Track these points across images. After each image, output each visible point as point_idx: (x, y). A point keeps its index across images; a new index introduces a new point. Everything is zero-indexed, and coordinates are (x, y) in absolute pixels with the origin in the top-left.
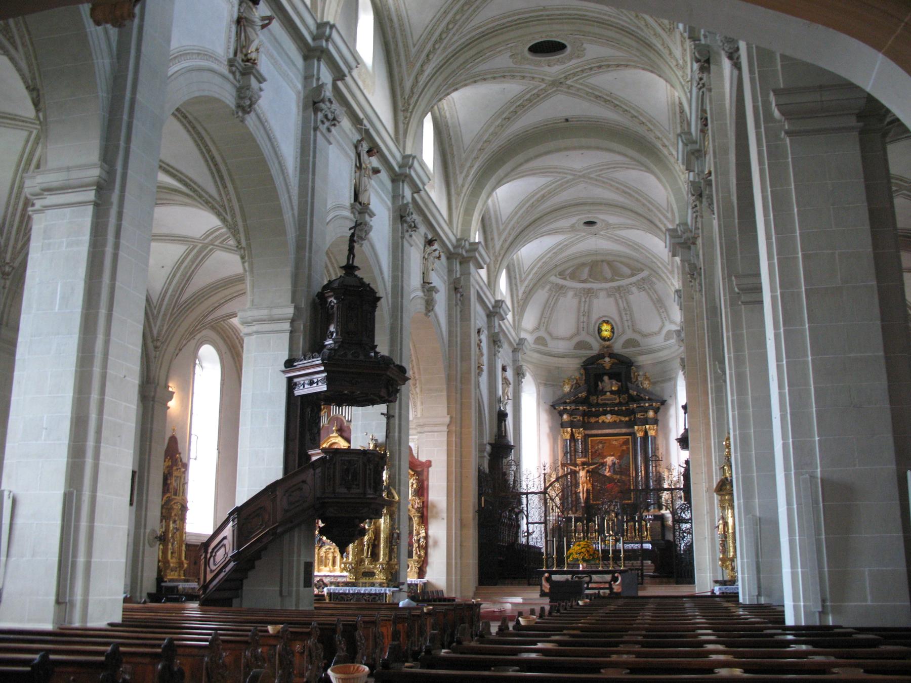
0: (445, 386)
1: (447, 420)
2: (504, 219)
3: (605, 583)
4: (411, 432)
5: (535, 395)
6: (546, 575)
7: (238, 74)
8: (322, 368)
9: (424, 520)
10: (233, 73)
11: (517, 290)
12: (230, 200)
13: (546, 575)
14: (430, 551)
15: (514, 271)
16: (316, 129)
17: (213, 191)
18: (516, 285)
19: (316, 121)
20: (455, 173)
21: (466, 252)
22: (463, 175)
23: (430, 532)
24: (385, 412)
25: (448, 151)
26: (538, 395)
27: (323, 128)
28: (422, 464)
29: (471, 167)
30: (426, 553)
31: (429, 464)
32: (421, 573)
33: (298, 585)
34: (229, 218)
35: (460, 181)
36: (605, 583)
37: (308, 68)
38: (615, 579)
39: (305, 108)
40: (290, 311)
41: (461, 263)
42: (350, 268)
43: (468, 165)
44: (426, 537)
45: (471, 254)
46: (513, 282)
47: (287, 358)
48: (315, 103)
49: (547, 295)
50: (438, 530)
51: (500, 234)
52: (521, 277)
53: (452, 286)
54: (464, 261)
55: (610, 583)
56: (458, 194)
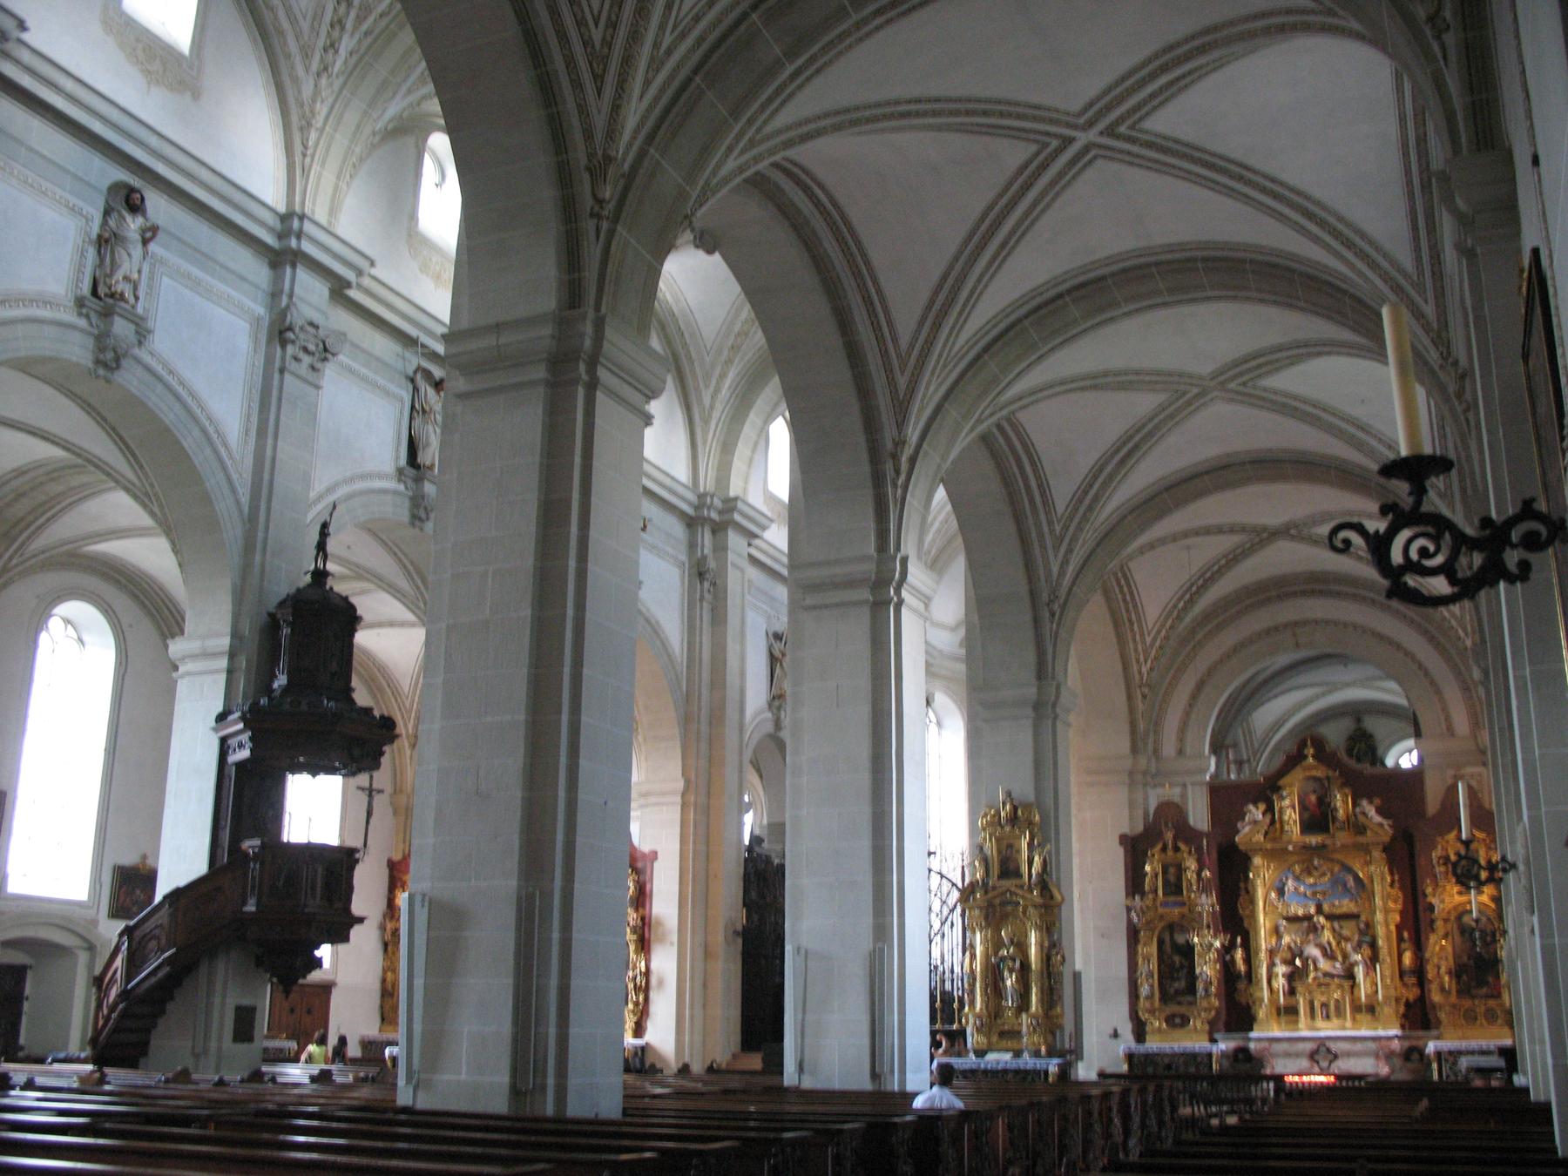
0: (676, 731)
1: (680, 785)
4: (633, 805)
7: (93, 316)
8: (241, 726)
9: (644, 945)
10: (87, 317)
12: (152, 486)
14: (652, 995)
16: (282, 371)
17: (130, 475)
19: (283, 359)
20: (697, 388)
21: (720, 513)
22: (712, 389)
23: (654, 965)
24: (367, 785)
25: (682, 352)
27: (303, 369)
28: (644, 855)
29: (722, 376)
30: (646, 999)
31: (654, 856)
32: (639, 1031)
33: (220, 1039)
34: (156, 510)
35: (707, 401)
37: (277, 281)
39: (269, 341)
40: (225, 642)
41: (714, 532)
42: (320, 576)
43: (717, 372)
44: (647, 974)
45: (726, 517)
47: (220, 709)
48: (281, 332)
50: (664, 962)
53: (695, 570)
54: (719, 529)
56: (706, 422)
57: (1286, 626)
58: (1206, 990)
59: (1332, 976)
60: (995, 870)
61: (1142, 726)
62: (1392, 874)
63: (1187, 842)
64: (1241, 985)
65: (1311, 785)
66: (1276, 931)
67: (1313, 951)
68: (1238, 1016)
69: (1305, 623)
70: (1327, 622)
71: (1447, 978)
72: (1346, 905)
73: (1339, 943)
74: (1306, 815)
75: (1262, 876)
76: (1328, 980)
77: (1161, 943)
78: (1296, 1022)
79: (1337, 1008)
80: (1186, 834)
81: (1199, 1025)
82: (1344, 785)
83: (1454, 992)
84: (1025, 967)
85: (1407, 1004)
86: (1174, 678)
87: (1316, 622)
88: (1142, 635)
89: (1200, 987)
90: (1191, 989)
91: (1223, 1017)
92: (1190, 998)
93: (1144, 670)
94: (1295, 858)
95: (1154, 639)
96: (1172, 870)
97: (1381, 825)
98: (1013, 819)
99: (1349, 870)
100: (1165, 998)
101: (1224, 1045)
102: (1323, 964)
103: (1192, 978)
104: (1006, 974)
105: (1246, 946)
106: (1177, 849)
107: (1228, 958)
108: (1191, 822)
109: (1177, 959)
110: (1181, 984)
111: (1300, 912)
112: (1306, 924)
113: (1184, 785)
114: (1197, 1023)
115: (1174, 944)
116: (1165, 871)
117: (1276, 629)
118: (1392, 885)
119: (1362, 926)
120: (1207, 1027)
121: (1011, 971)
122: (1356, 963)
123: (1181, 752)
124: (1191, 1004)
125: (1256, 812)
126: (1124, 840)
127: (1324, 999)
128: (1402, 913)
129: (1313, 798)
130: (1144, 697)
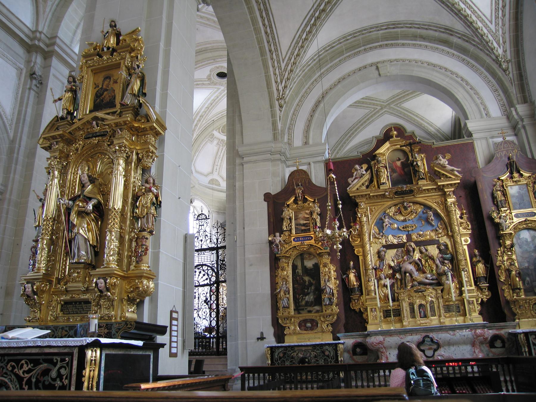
45: (50, 49)
49: (216, 149)
54: (47, 55)
57: (371, 65)
58: (330, 299)
59: (425, 284)
61: (279, 125)
62: (461, 209)
63: (311, 196)
64: (355, 297)
66: (380, 256)
70: (397, 60)
71: (517, 279)
72: (429, 234)
73: (426, 261)
74: (395, 175)
75: (367, 216)
76: (422, 287)
77: (294, 267)
79: (432, 308)
80: (310, 188)
81: (324, 326)
82: (420, 152)
83: (522, 290)
85: (482, 303)
88: (279, 62)
89: (325, 297)
90: (318, 301)
91: (343, 321)
92: (317, 308)
93: (280, 88)
95: (287, 65)
97: (453, 170)
99: (430, 208)
100: (298, 309)
103: (319, 291)
105: (357, 267)
106: (305, 200)
107: (344, 277)
108: (314, 182)
109: (307, 279)
110: (310, 298)
111: (395, 241)
113: (309, 164)
115: (304, 268)
117: (365, 67)
118: (461, 218)
119: (443, 247)
120: (330, 328)
122: (445, 273)
123: (306, 143)
124: (317, 311)
126: (267, 197)
128: (472, 236)
129: (399, 163)
130: (281, 106)
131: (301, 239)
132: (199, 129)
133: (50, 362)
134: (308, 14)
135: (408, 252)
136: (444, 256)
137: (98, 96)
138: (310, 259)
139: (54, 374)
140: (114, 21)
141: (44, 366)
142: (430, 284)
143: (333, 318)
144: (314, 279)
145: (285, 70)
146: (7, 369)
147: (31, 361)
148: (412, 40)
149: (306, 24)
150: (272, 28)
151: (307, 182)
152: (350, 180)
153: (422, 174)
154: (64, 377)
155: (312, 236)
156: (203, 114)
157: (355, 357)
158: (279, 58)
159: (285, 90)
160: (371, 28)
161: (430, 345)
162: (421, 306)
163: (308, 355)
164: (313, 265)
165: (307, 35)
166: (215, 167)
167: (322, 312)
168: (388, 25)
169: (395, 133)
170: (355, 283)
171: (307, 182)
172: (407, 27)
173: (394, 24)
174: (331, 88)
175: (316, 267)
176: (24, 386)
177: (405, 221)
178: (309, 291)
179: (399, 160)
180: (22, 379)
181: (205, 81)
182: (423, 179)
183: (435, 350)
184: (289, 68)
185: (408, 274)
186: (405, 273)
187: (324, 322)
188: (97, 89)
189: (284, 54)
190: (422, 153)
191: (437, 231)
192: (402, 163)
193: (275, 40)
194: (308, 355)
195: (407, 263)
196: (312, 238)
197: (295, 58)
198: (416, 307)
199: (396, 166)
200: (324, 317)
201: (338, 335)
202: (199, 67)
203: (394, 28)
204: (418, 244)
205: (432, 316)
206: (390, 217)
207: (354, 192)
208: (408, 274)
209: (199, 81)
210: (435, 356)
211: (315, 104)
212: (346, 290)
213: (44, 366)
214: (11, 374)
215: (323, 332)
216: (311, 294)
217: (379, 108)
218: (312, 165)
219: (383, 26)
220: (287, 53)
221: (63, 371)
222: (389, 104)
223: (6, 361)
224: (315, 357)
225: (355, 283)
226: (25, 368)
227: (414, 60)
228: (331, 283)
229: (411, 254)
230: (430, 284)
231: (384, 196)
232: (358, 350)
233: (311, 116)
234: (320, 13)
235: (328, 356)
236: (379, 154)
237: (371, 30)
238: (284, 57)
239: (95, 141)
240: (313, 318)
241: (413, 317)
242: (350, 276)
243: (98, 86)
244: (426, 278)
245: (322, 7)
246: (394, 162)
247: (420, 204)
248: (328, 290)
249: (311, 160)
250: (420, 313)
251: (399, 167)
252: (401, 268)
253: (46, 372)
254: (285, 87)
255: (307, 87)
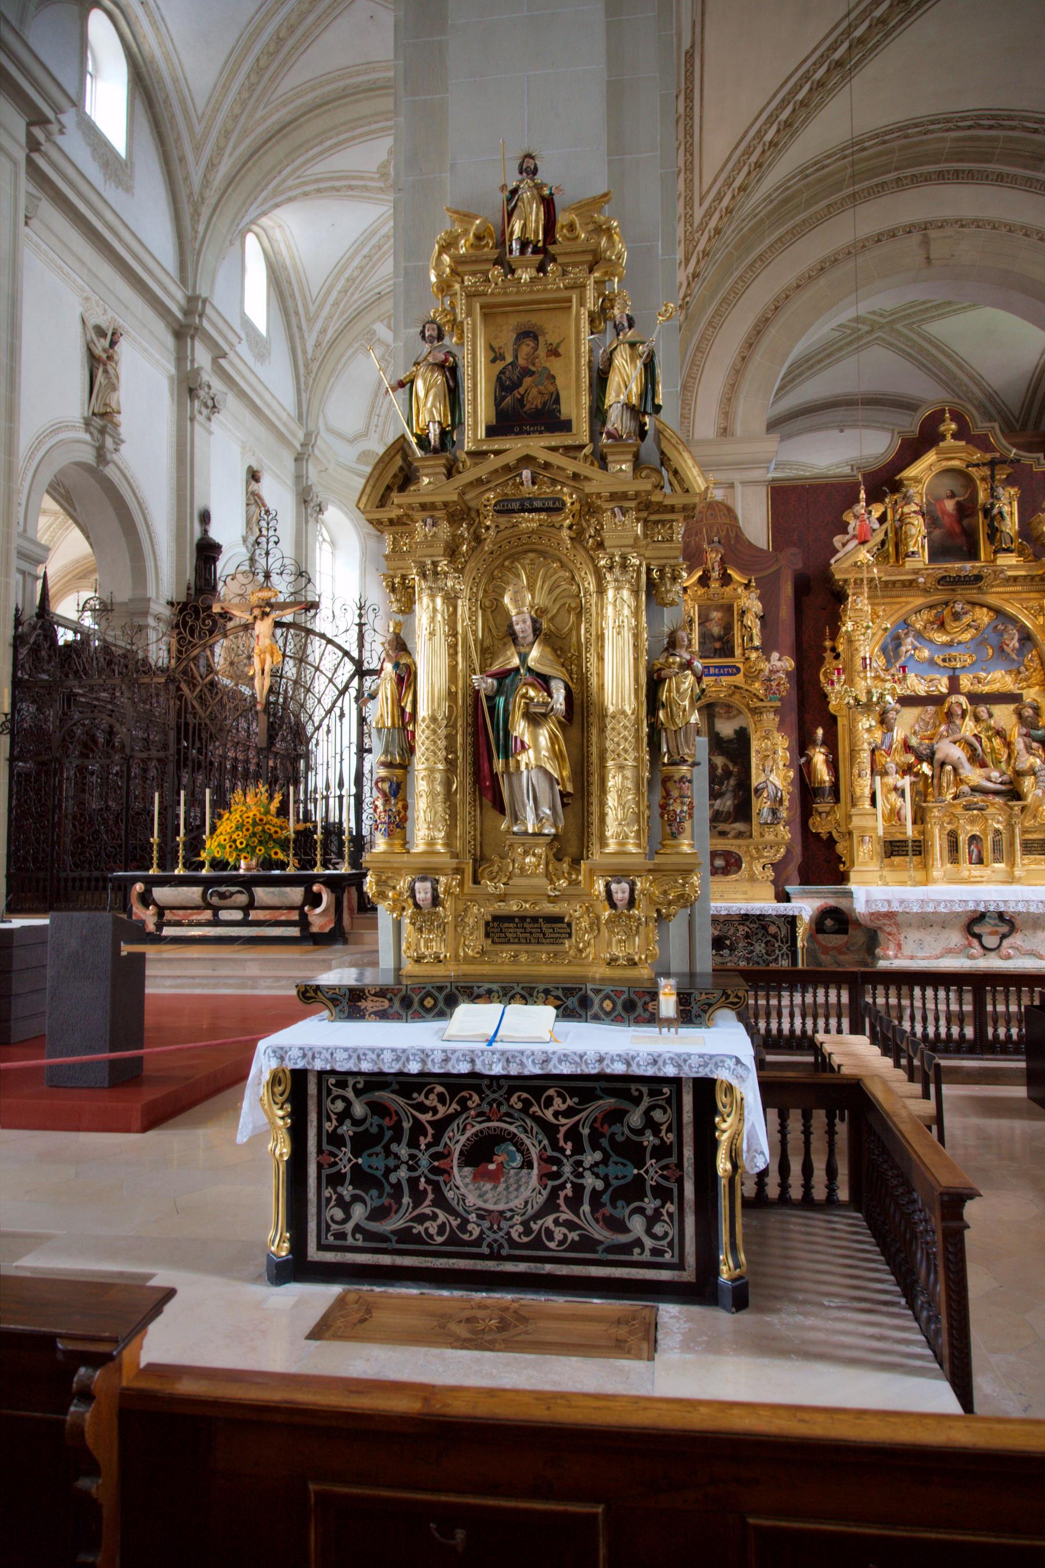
2: (201, 103)
3: (291, 908)
5: (358, 554)
6: (139, 887)
11: (302, 338)
13: (139, 887)
15: (292, 296)
18: (300, 329)
26: (364, 554)
36: (291, 908)
38: (314, 900)
46: (294, 322)
51: (198, 148)
52: (307, 312)
55: (301, 908)
57: (909, 230)
58: (774, 812)
59: (985, 792)
60: (479, 408)
63: (743, 569)
64: (822, 806)
65: (949, 484)
67: (951, 751)
68: (822, 861)
69: (942, 225)
70: (977, 223)
72: (999, 680)
74: (937, 533)
75: (863, 626)
76: (978, 798)
78: (925, 866)
79: (997, 846)
81: (757, 868)
82: (1010, 481)
84: (581, 714)
86: (717, 313)
87: (962, 224)
89: (761, 806)
92: (739, 826)
94: (920, 601)
95: (709, 214)
96: (716, 615)
98: (543, 250)
101: (805, 906)
102: (973, 775)
104: (521, 728)
105: (831, 743)
111: (921, 689)
112: (931, 709)
113: (731, 486)
114: (758, 868)
116: (704, 620)
117: (892, 234)
119: (1028, 712)
120: (770, 873)
121: (535, 719)
123: (725, 432)
124: (740, 835)
125: (865, 515)
127: (976, 830)
129: (950, 505)
131: (712, 671)
132: (342, 314)
133: (624, 1094)
134: (796, 70)
135: (949, 715)
136: (1033, 732)
137: (505, 386)
138: (729, 718)
139: (635, 1119)
140: (529, 156)
141: (609, 1102)
142: (996, 793)
143: (778, 851)
144: (735, 763)
145: (702, 227)
146: (512, 1107)
147: (573, 1092)
148: (1026, 167)
149: (783, 100)
150: (692, 101)
151: (732, 535)
152: (837, 540)
153: (1008, 540)
154: (664, 1128)
155: (740, 665)
156: (356, 273)
157: (820, 937)
158: (692, 191)
159: (693, 285)
160: (932, 123)
161: (996, 925)
162: (973, 838)
163: (731, 932)
164: (736, 732)
165: (778, 131)
166: (375, 420)
167: (751, 836)
168: (980, 117)
169: (953, 426)
170: (827, 778)
171: (732, 535)
172: (1026, 129)
173: (994, 117)
174: (798, 286)
175: (743, 737)
176: (561, 1143)
177: (949, 645)
178: (724, 788)
179: (952, 495)
180: (556, 1128)
181: (372, 179)
182: (1008, 550)
183: (1004, 937)
184: (712, 224)
185: (949, 768)
186: (943, 764)
187: (758, 858)
188: (500, 365)
189: (708, 179)
190: (1013, 486)
191: (1019, 673)
192: (958, 503)
193: (692, 137)
194: (731, 932)
195: (946, 741)
196: (738, 670)
197: (733, 197)
198: (963, 839)
199: (944, 512)
200: (757, 849)
201: (789, 888)
202: (362, 135)
203: (991, 127)
204: (975, 699)
205: (997, 860)
206: (919, 635)
207: (846, 571)
208: (949, 768)
209: (354, 178)
210: (1002, 948)
211: (754, 328)
212: (807, 792)
213: (609, 1102)
214: (523, 1116)
215: (752, 879)
216: (729, 795)
217: (865, 328)
218: (739, 488)
219: (963, 119)
220: (715, 181)
221: (658, 1115)
222: (890, 322)
223: (504, 1090)
224: (747, 936)
225: (827, 778)
226: (558, 1104)
227: (1022, 228)
228: (773, 773)
229: (958, 722)
230: (996, 793)
231: (910, 584)
232: (829, 922)
233: (744, 358)
234: (828, 70)
235: (775, 936)
236: (908, 479)
237: (931, 127)
238: (705, 187)
239: (529, 521)
240: (733, 849)
241: (954, 859)
242: (815, 760)
243: (503, 358)
244: (989, 779)
245: (837, 56)
246: (939, 500)
247: (990, 608)
248: (771, 788)
249: (736, 476)
250: (970, 853)
251: (949, 515)
252: (933, 753)
253: (616, 1116)
254: (695, 276)
255: (737, 274)
